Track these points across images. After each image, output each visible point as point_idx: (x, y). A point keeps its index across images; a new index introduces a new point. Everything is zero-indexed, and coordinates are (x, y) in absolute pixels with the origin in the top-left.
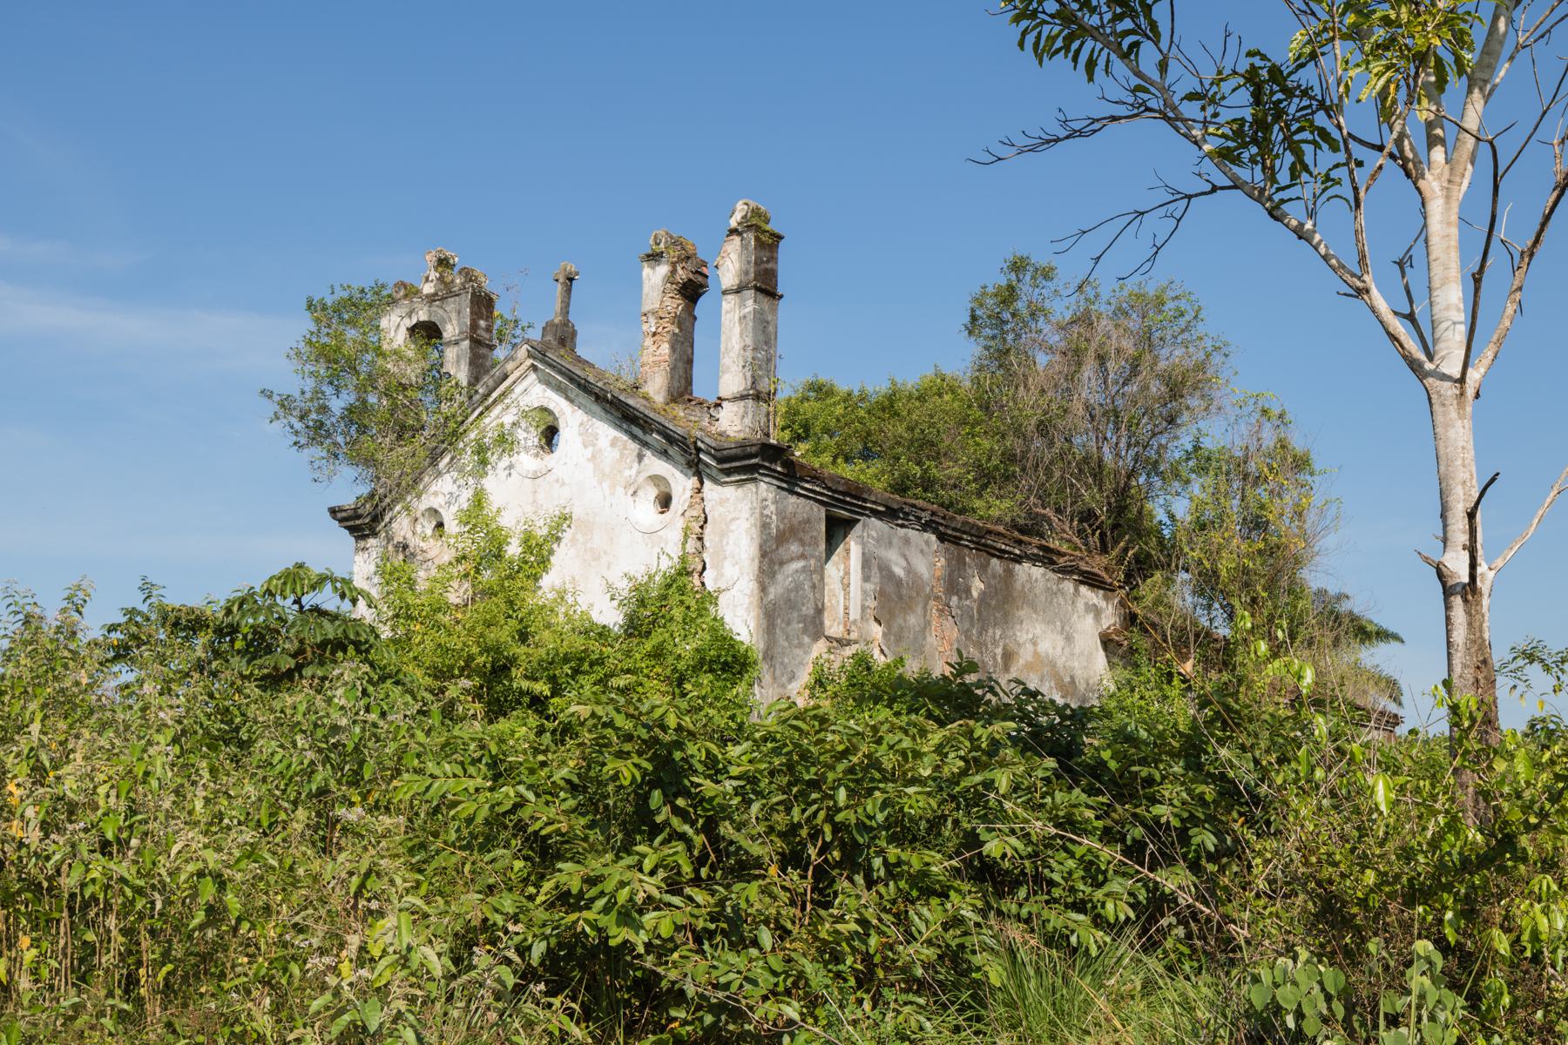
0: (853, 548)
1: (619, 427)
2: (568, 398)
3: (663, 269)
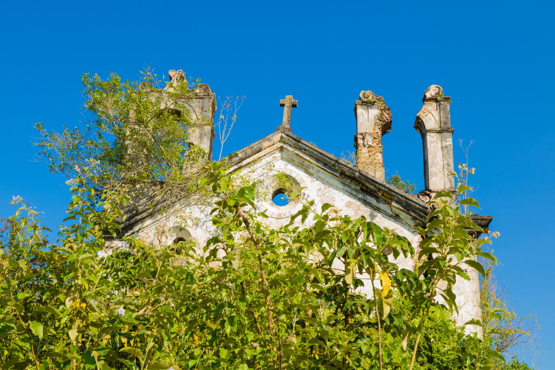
1: (351, 195)
2: (307, 172)
3: (374, 112)
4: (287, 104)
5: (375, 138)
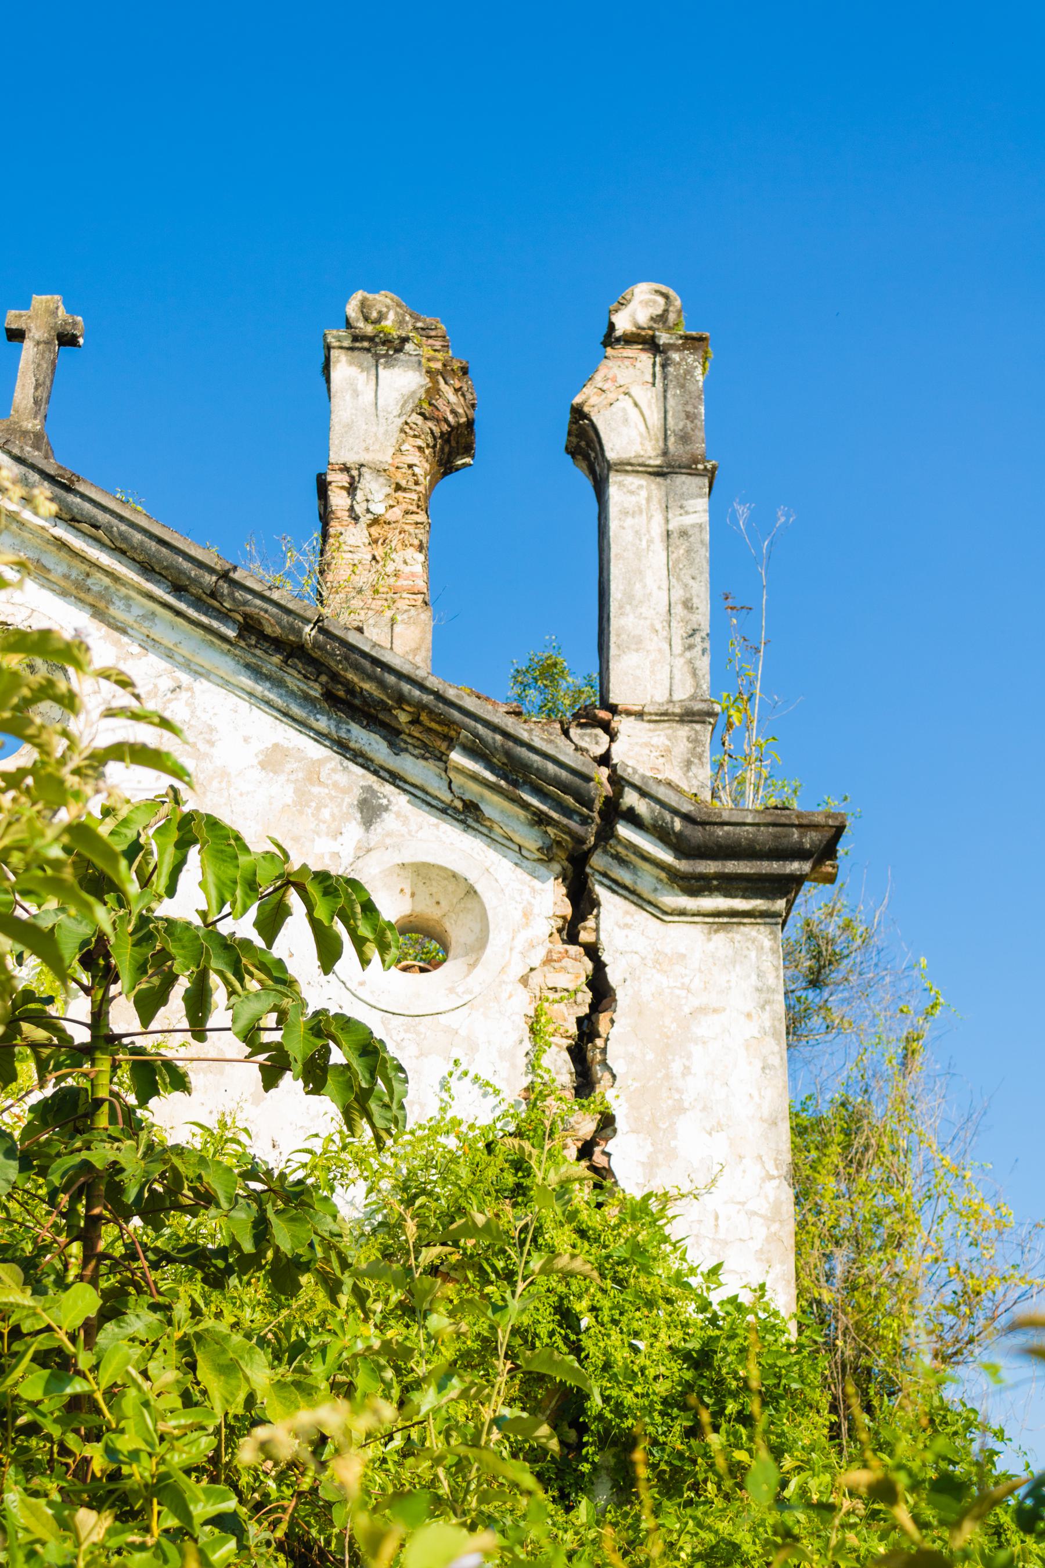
3: (402, 381)
4: (37, 332)
5: (398, 488)
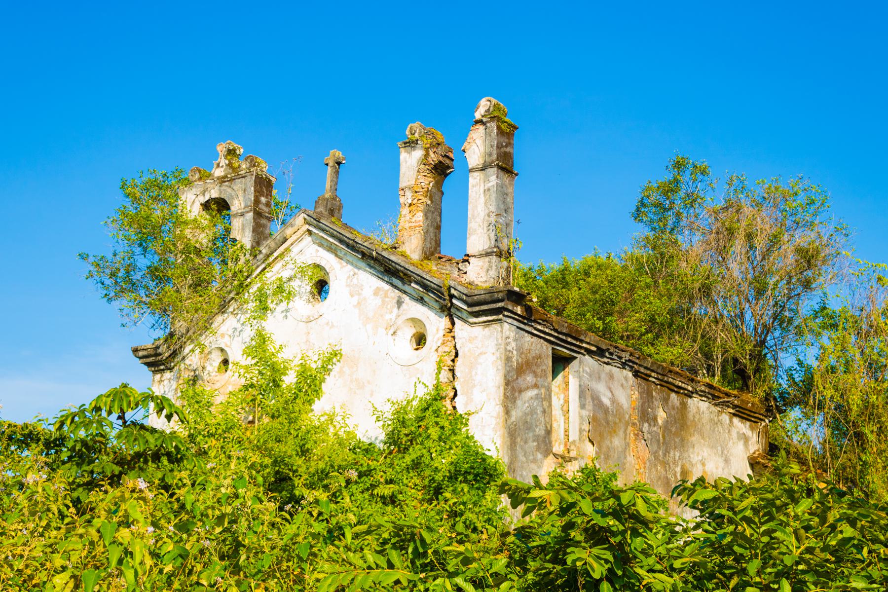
0: (572, 378)
2: (336, 255)
3: (418, 153)
